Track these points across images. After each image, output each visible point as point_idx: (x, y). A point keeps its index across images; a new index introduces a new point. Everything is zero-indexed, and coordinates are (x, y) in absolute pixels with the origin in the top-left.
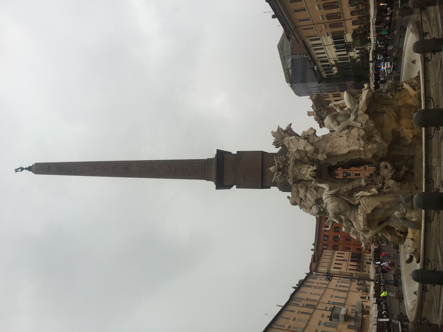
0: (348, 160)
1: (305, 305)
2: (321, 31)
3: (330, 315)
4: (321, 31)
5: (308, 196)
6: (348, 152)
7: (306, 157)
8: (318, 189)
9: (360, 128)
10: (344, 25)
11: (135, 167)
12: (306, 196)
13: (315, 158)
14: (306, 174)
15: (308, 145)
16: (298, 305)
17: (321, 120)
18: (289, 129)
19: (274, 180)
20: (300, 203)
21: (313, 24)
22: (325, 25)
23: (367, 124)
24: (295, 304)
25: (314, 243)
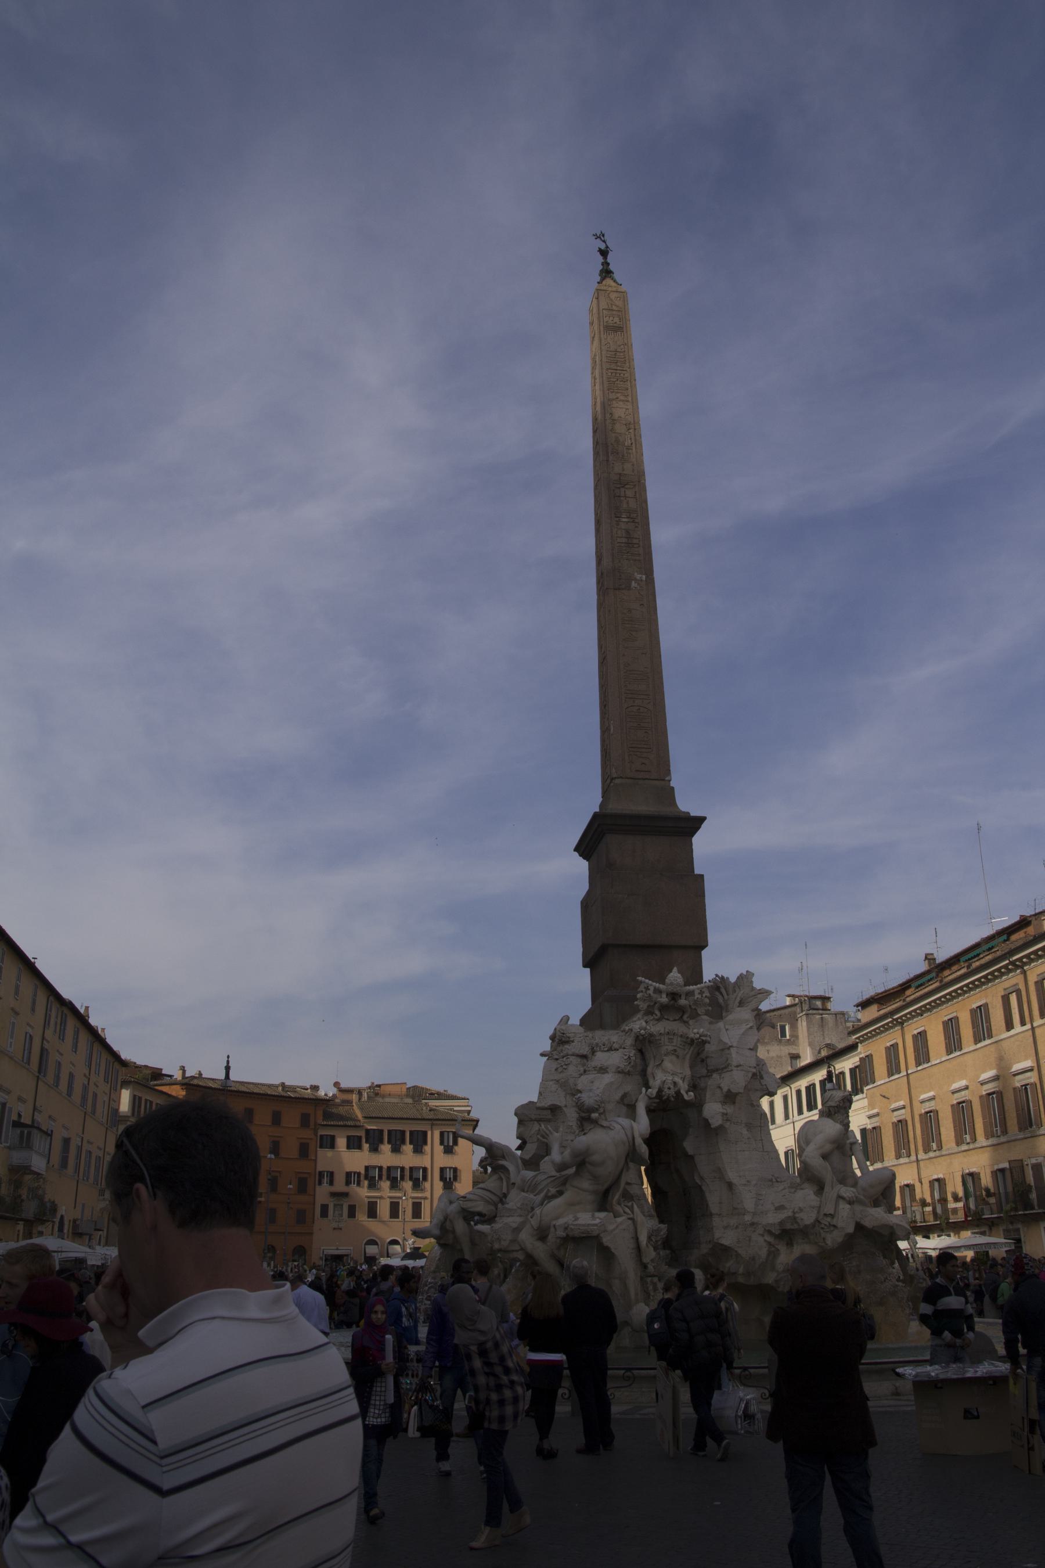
0: (700, 1184)
1: (46, 1045)
2: (884, 1097)
3: (22, 1121)
4: (884, 1097)
5: (608, 1078)
6: (730, 1185)
7: (704, 1072)
8: (624, 1104)
9: (818, 1212)
10: (902, 1160)
11: (636, 574)
12: (603, 1070)
13: (708, 1096)
14: (665, 1071)
15: (747, 1076)
16: (46, 1023)
17: (830, 1111)
18: (761, 1020)
19: (644, 982)
20: (573, 1055)
21: (909, 1072)
22: (904, 1107)
23: (832, 1228)
24: (50, 1015)
25: (203, 1076)
